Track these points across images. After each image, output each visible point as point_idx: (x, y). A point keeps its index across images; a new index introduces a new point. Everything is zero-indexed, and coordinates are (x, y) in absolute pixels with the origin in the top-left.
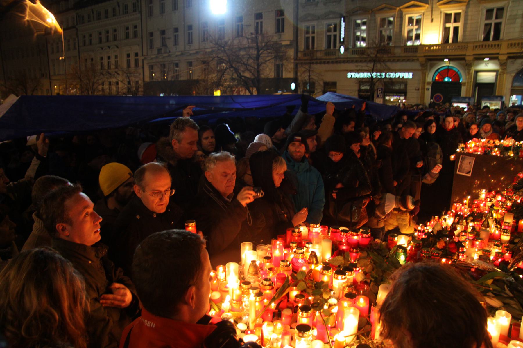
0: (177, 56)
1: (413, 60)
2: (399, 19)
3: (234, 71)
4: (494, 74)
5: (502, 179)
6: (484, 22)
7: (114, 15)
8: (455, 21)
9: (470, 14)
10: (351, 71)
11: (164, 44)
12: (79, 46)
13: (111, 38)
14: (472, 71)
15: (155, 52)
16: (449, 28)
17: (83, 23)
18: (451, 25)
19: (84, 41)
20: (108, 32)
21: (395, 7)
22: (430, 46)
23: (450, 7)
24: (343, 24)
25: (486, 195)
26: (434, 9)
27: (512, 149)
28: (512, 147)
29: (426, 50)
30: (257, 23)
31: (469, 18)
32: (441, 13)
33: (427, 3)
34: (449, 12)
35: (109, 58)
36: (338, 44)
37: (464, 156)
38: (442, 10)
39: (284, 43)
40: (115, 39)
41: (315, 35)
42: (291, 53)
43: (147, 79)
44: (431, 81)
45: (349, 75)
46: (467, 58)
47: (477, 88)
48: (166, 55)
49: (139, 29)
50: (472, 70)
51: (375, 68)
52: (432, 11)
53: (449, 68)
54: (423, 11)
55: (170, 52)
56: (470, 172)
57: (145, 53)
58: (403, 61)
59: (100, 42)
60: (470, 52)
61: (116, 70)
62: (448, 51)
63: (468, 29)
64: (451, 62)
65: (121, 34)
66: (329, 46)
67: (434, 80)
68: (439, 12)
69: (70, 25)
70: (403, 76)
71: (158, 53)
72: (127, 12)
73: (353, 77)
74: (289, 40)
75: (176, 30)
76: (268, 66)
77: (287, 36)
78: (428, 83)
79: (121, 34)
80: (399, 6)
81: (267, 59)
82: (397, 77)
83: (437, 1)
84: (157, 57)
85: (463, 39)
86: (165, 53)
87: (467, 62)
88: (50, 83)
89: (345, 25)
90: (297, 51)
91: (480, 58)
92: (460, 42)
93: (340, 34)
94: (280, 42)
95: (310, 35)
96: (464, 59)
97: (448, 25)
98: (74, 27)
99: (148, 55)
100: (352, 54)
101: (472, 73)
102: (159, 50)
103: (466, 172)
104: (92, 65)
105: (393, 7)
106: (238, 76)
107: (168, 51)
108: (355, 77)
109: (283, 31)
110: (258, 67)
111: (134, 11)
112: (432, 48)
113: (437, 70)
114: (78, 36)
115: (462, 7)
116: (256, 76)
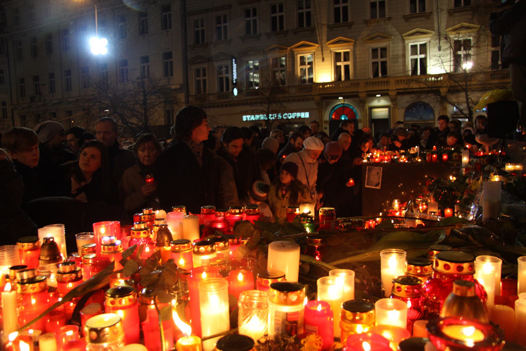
0: (53, 104)
1: (308, 100)
2: (291, 59)
3: (118, 117)
4: (386, 110)
6: (371, 61)
8: (345, 60)
9: (357, 52)
10: (246, 114)
11: (38, 91)
14: (367, 108)
16: (340, 66)
18: (342, 64)
21: (286, 47)
22: (324, 84)
23: (339, 47)
24: (235, 65)
25: (399, 204)
26: (324, 48)
27: (418, 155)
28: (418, 153)
29: (320, 89)
30: (144, 67)
31: (358, 56)
32: (331, 52)
33: (317, 43)
34: (338, 51)
36: (231, 86)
37: (370, 167)
38: (332, 49)
39: (173, 87)
41: (206, 78)
42: (182, 97)
44: (328, 119)
45: (245, 118)
46: (361, 95)
47: (373, 124)
50: (366, 107)
51: (270, 110)
52: (322, 51)
53: (345, 105)
54: (313, 51)
55: (45, 100)
56: (378, 184)
58: (299, 100)
60: (362, 89)
62: (341, 89)
63: (358, 67)
64: (346, 100)
66: (222, 89)
67: (330, 119)
68: (329, 51)
70: (300, 116)
73: (248, 120)
74: (178, 84)
75: (52, 75)
76: (156, 111)
77: (177, 79)
78: (326, 122)
80: (290, 47)
81: (155, 104)
82: (294, 117)
83: (326, 41)
85: (354, 77)
87: (361, 99)
89: (237, 66)
90: (188, 95)
91: (372, 95)
92: (352, 80)
93: (233, 75)
94: (168, 87)
95: (201, 78)
96: (357, 96)
97: (339, 64)
100: (247, 96)
101: (366, 109)
102: (32, 99)
103: (375, 185)
105: (284, 47)
106: (123, 122)
108: (251, 120)
109: (172, 75)
110: (146, 113)
112: (326, 86)
113: (333, 109)
115: (350, 47)
116: (144, 122)
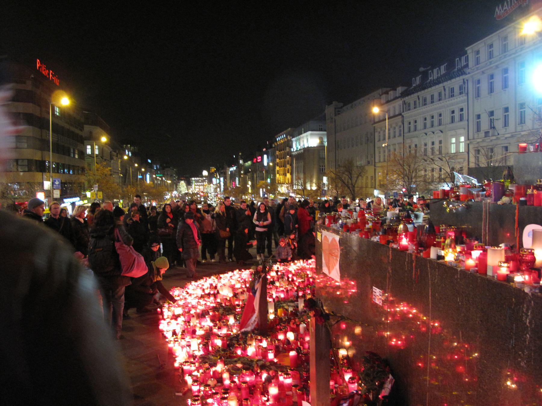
0: (506, 138)
5: (476, 354)
7: (440, 100)
12: (404, 133)
13: (436, 123)
15: (482, 134)
17: (409, 110)
19: (409, 128)
20: (433, 117)
35: (433, 143)
40: (440, 124)
43: (472, 165)
48: (494, 138)
49: (465, 112)
55: (498, 134)
57: (471, 137)
59: (425, 127)
61: (440, 156)
65: (446, 118)
69: (397, 113)
71: (485, 137)
72: (453, 95)
75: (506, 110)
79: (446, 118)
84: (483, 141)
86: (493, 135)
88: (375, 169)
98: (400, 114)
99: (474, 139)
102: (487, 133)
104: (416, 151)
107: (497, 134)
111: (461, 93)
114: (403, 124)
